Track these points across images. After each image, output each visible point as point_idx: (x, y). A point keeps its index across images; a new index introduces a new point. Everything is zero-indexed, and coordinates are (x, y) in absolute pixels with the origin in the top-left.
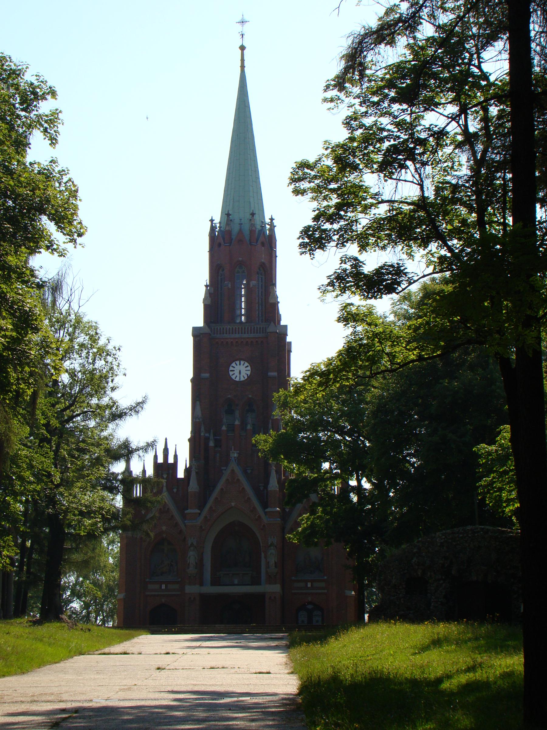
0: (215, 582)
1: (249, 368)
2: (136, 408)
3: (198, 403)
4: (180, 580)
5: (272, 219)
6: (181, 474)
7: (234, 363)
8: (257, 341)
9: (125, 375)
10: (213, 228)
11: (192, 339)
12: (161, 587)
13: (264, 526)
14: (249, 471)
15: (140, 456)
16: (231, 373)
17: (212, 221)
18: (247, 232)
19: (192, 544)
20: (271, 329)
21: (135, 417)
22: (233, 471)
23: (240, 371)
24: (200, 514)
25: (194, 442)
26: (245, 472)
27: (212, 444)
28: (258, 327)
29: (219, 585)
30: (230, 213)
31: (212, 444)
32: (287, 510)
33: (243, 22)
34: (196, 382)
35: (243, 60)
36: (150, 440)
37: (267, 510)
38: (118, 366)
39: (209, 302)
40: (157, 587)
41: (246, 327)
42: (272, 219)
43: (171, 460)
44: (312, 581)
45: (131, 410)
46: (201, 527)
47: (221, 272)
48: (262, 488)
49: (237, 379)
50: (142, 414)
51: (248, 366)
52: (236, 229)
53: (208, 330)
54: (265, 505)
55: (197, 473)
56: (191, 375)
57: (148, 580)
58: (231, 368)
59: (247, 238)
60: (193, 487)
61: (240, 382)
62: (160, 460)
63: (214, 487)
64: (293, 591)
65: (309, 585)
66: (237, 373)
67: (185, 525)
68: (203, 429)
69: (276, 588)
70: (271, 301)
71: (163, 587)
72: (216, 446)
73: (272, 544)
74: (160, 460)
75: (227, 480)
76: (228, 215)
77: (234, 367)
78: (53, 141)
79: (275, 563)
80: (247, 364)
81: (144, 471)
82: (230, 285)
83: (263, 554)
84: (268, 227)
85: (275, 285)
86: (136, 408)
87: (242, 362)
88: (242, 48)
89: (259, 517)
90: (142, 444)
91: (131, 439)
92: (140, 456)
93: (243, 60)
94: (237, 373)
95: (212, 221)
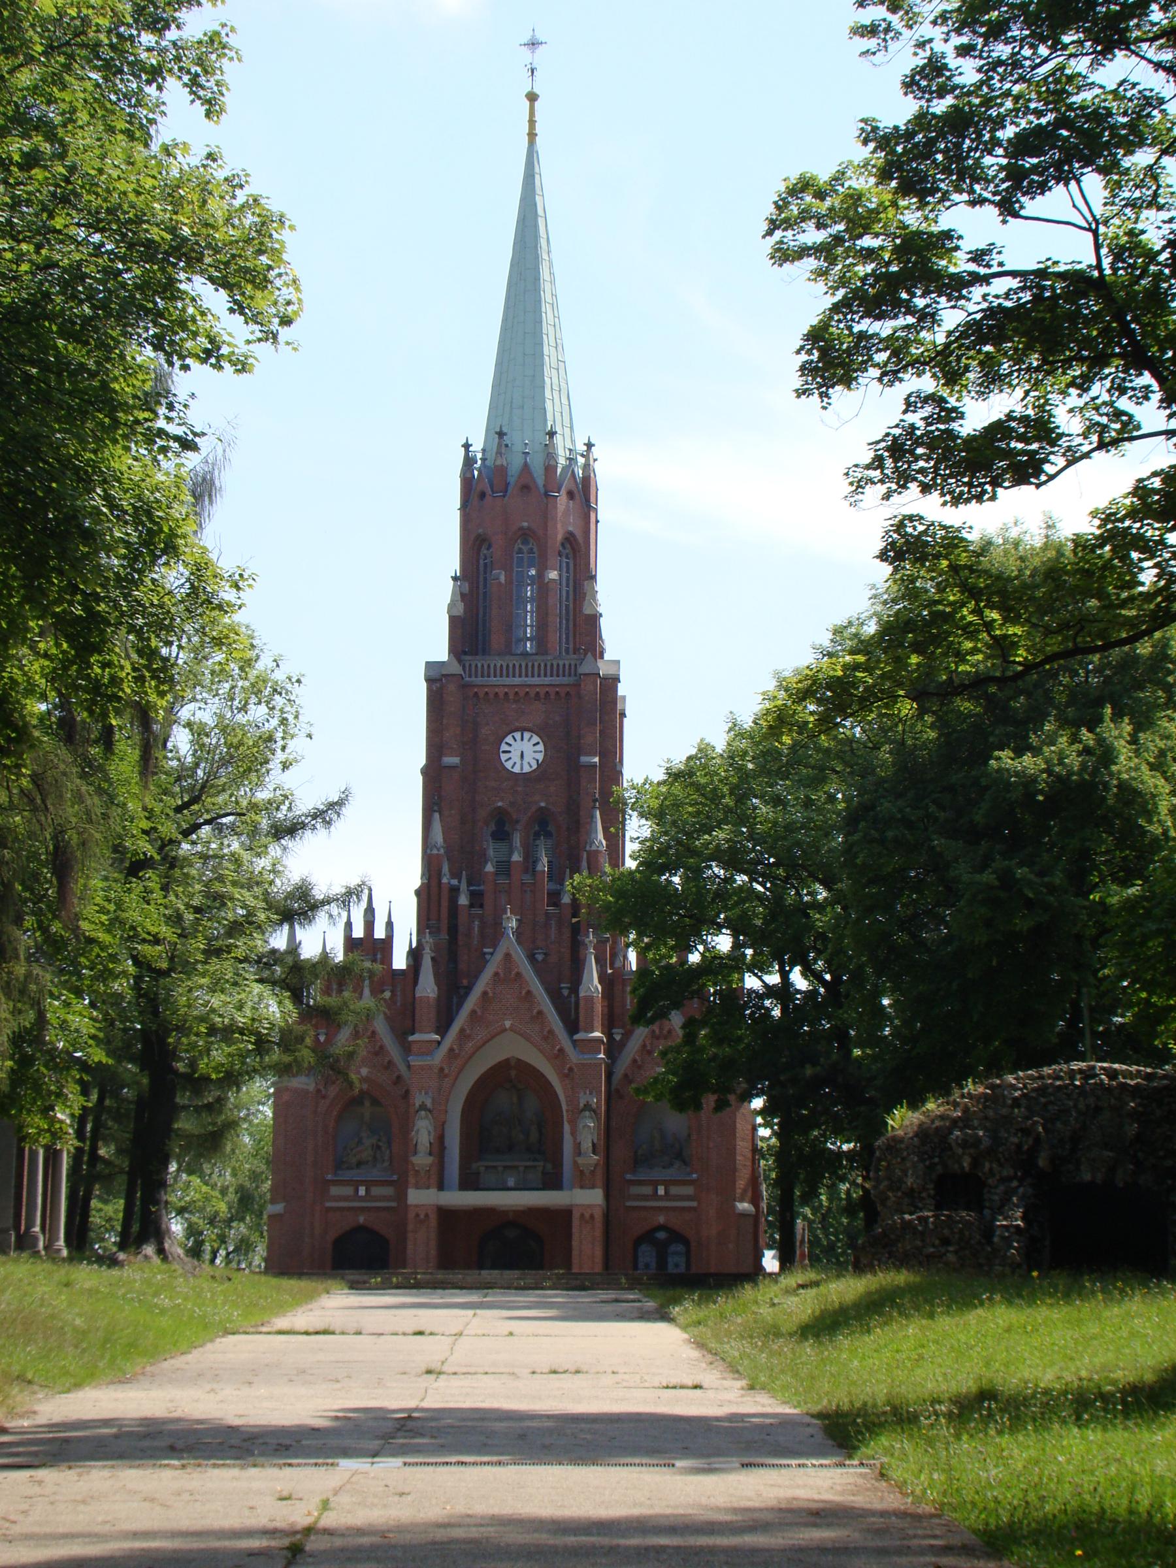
0: (469, 1182)
1: (541, 747)
2: (325, 815)
3: (437, 815)
4: (395, 1177)
5: (589, 446)
6: (400, 961)
9: (310, 736)
10: (469, 462)
11: (424, 685)
12: (357, 1191)
13: (571, 1069)
14: (540, 957)
15: (331, 916)
16: (504, 757)
17: (467, 446)
19: (423, 1107)
20: (584, 669)
21: (322, 832)
22: (508, 956)
23: (523, 753)
24: (439, 1043)
25: (428, 897)
26: (531, 958)
27: (463, 900)
29: (477, 1188)
30: (505, 430)
31: (463, 900)
32: (618, 1038)
33: (533, 44)
34: (433, 775)
35: (532, 122)
36: (353, 882)
37: (576, 1037)
38: (296, 717)
39: (460, 610)
40: (348, 1191)
42: (589, 446)
43: (380, 933)
44: (667, 1184)
45: (315, 817)
46: (441, 1069)
47: (484, 551)
48: (566, 992)
49: (517, 770)
50: (339, 826)
52: (515, 464)
53: (456, 669)
54: (573, 1027)
55: (433, 959)
56: (422, 761)
57: (329, 1177)
58: (504, 747)
59: (540, 481)
60: (428, 987)
62: (358, 932)
63: (469, 989)
64: (628, 1204)
65: (661, 1191)
66: (515, 757)
67: (409, 1067)
68: (446, 869)
69: (593, 1197)
70: (587, 611)
71: (362, 1191)
72: (471, 905)
73: (587, 1107)
74: (358, 932)
75: (496, 974)
76: (501, 434)
78: (213, 108)
79: (594, 1145)
80: (536, 739)
82: (502, 579)
83: (567, 1127)
84: (581, 460)
85: (593, 578)
86: (325, 815)
87: (527, 735)
88: (532, 97)
89: (561, 1050)
90: (338, 890)
91: (313, 880)
92: (331, 916)
93: (532, 122)
94: (515, 757)
95: (467, 446)
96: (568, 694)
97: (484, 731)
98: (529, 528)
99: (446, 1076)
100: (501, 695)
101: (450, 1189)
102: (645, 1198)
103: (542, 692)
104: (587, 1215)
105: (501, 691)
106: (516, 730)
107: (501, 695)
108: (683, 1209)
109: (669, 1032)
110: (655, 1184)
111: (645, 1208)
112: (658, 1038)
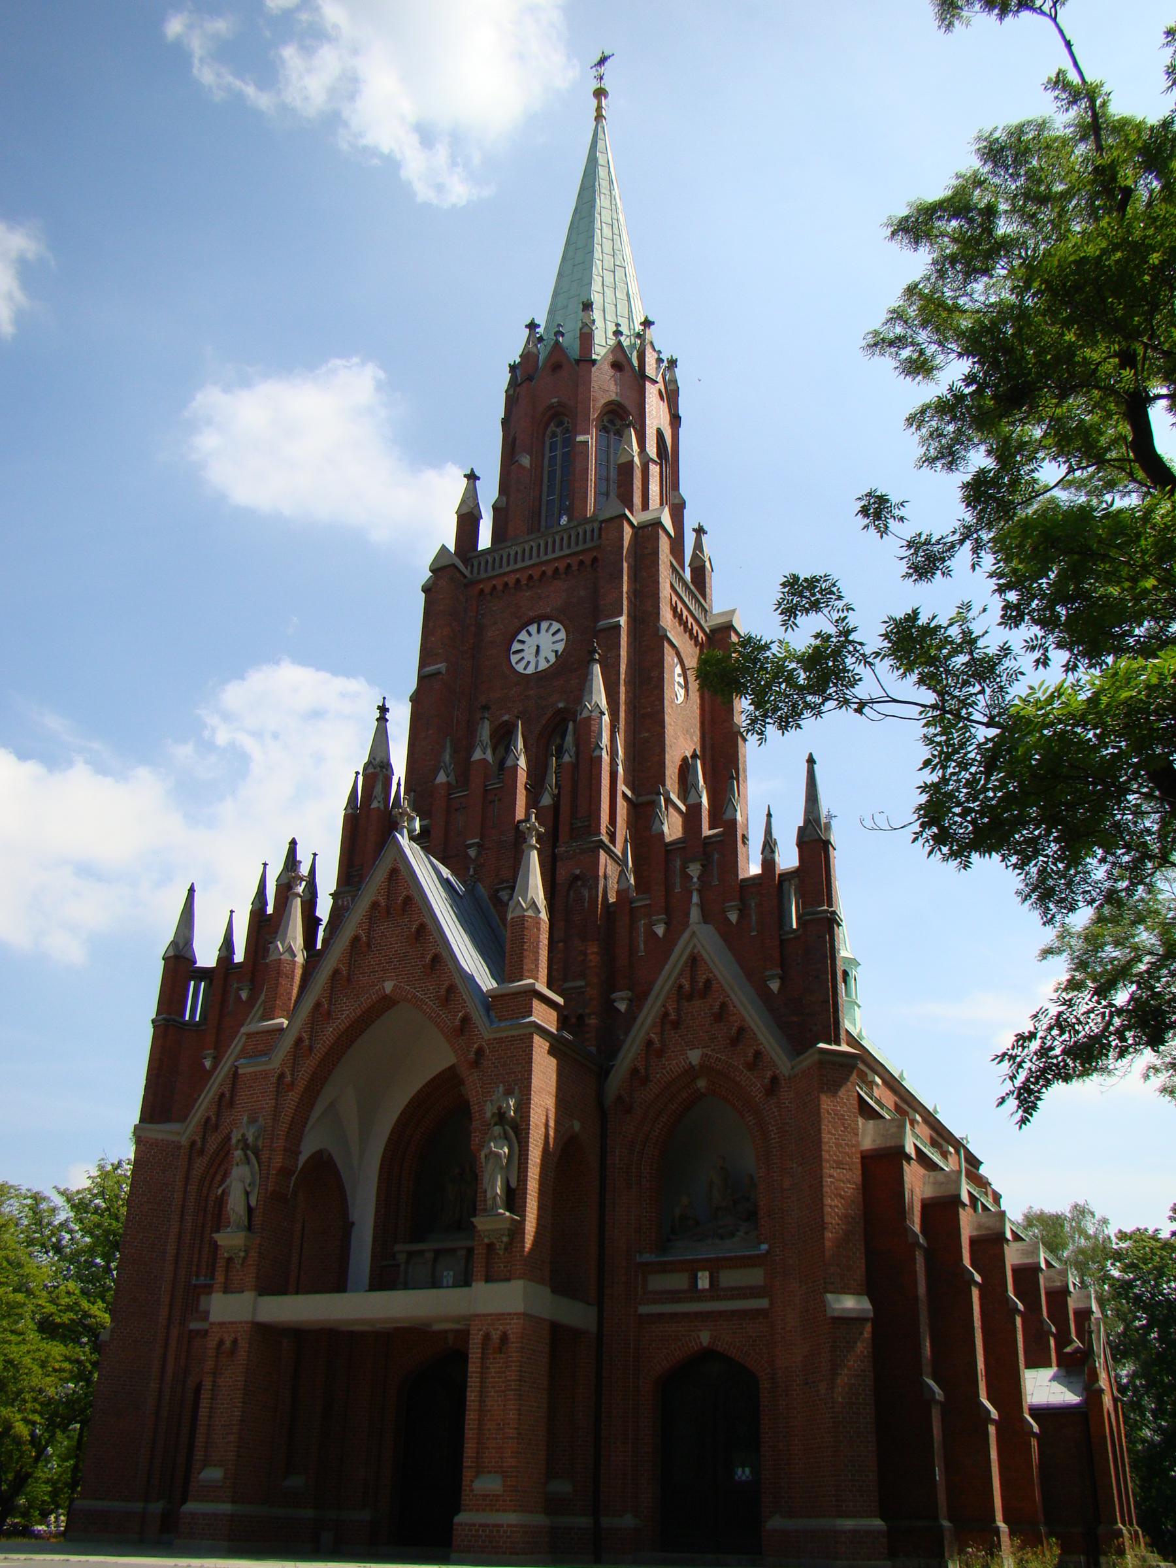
1: (562, 635)
7: (524, 632)
8: (581, 563)
13: (480, 1052)
16: (514, 659)
18: (570, 342)
28: (588, 527)
32: (622, 1007)
33: (603, 61)
41: (557, 538)
44: (715, 1266)
46: (282, 1076)
51: (559, 630)
61: (539, 676)
64: (643, 1309)
65: (704, 1282)
66: (529, 654)
75: (375, 905)
77: (523, 642)
80: (556, 626)
87: (544, 625)
93: (599, 108)
96: (595, 560)
98: (560, 404)
101: (355, 1290)
102: (674, 1296)
103: (561, 566)
104: (496, 1336)
106: (530, 623)
109: (708, 983)
110: (692, 1269)
111: (674, 1316)
112: (690, 997)
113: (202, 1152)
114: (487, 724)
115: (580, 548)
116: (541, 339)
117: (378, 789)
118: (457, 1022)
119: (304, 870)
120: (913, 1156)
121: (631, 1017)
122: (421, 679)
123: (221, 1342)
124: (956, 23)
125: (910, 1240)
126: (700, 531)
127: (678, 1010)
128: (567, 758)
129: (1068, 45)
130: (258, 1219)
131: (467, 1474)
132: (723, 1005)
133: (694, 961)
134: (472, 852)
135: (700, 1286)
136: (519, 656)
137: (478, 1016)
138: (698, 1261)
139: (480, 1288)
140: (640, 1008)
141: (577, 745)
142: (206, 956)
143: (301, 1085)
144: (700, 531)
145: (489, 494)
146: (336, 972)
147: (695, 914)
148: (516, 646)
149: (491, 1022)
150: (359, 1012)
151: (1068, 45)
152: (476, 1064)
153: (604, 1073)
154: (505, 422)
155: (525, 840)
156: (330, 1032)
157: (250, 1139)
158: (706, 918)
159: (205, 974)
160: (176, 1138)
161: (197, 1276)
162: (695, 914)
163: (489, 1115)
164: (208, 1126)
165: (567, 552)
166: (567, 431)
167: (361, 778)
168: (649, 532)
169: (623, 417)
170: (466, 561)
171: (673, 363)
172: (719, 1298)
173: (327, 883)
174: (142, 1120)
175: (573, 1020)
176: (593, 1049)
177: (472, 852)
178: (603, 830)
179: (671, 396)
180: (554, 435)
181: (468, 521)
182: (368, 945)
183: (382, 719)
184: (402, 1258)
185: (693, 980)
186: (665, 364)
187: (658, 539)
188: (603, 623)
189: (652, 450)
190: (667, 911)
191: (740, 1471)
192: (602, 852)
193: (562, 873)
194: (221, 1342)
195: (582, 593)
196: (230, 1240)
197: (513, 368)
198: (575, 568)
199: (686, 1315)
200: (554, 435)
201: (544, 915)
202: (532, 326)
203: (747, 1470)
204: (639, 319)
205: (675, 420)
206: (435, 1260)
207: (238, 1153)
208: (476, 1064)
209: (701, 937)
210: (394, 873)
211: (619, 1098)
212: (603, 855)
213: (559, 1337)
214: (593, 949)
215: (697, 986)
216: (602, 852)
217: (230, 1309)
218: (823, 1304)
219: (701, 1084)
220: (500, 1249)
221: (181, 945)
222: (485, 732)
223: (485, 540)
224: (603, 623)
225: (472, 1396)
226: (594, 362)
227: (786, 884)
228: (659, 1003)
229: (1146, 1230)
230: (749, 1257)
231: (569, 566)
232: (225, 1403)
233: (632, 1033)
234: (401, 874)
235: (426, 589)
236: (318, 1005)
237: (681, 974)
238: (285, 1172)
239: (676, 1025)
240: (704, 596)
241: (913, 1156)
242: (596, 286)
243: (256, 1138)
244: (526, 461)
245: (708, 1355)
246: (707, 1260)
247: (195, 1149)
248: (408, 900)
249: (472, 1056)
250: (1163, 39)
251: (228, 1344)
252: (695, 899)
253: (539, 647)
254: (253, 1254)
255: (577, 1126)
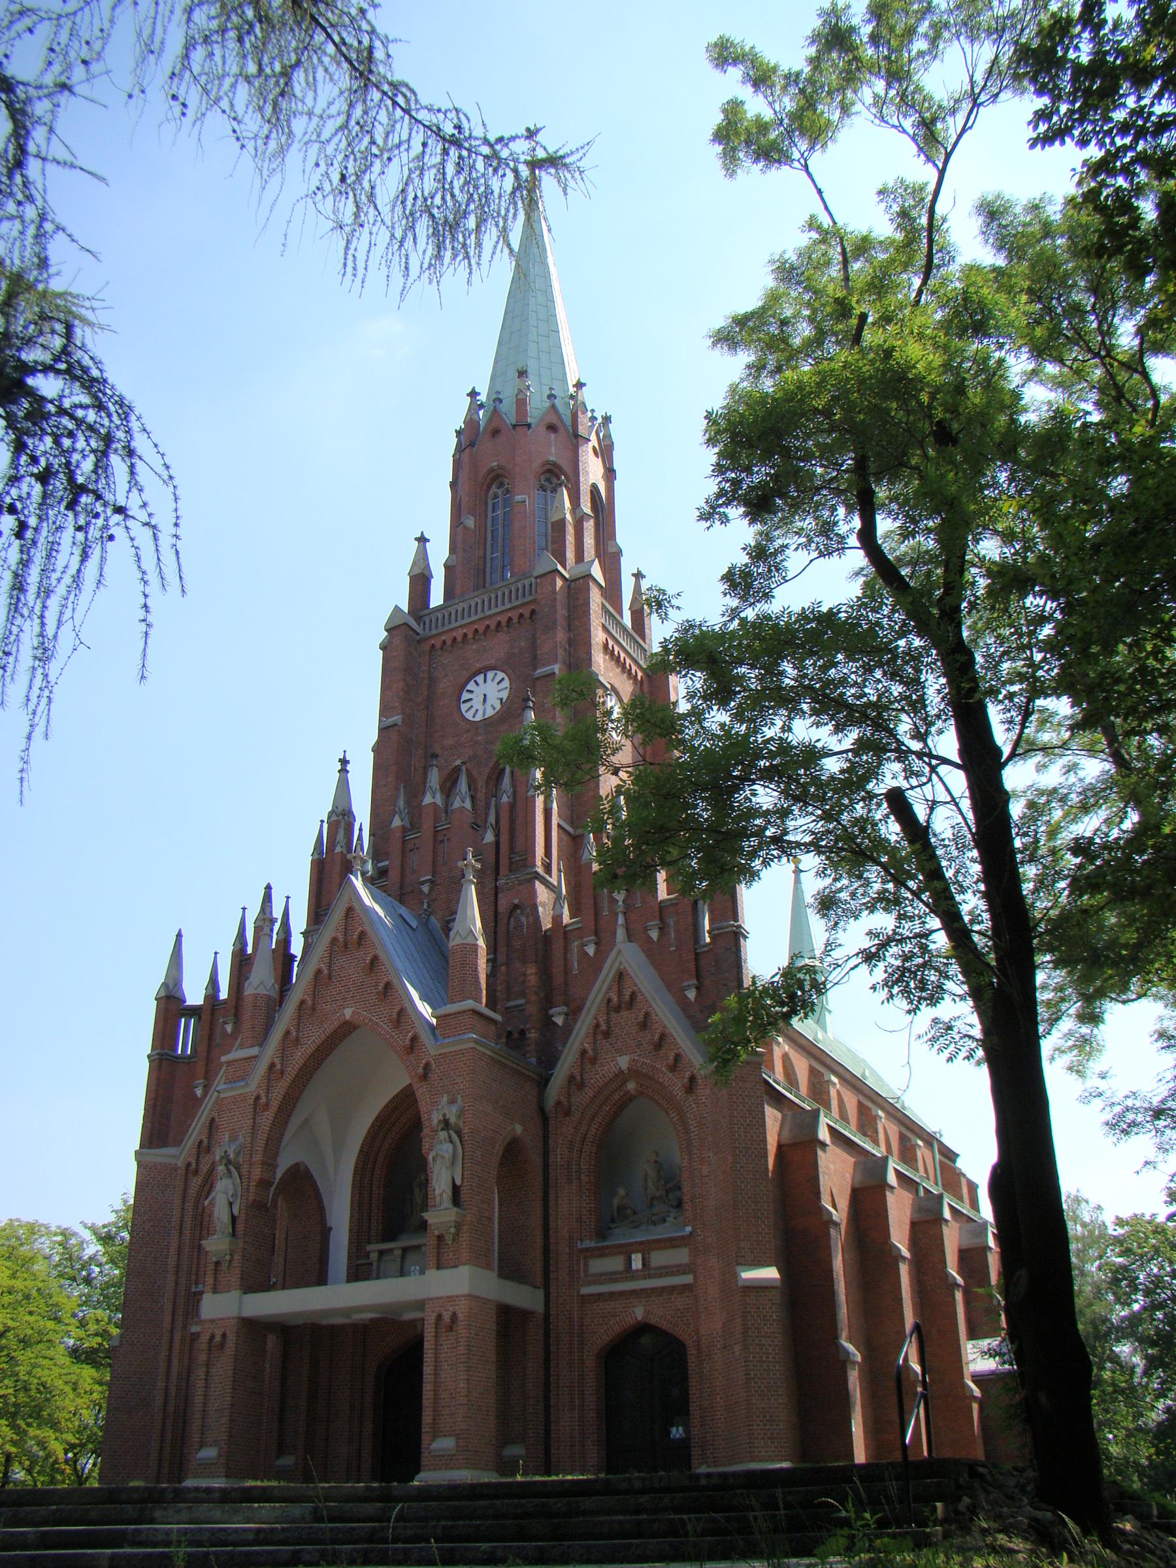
1: (506, 683)
7: (472, 682)
13: (427, 1066)
16: (464, 707)
18: (508, 408)
28: (527, 582)
32: (559, 1021)
41: (500, 593)
42: (579, 385)
46: (258, 1098)
49: (479, 718)
61: (487, 722)
64: (585, 1290)
65: (637, 1263)
66: (477, 703)
75: (334, 940)
77: (471, 692)
79: (456, 1189)
80: (501, 675)
81: (214, 982)
87: (490, 675)
96: (533, 612)
97: (443, 685)
98: (500, 467)
99: (267, 1106)
100: (459, 639)
102: (612, 1277)
103: (503, 619)
104: (447, 1317)
105: (458, 635)
107: (459, 639)
108: (672, 1289)
109: (633, 995)
110: (626, 1251)
111: (612, 1295)
112: (618, 1009)
113: (196, 1172)
114: (435, 770)
115: (518, 603)
116: (481, 406)
117: (341, 833)
118: (407, 1042)
119: (277, 913)
120: (828, 1141)
121: (568, 1029)
122: (382, 730)
123: (213, 1337)
124: (739, 171)
125: (825, 1218)
126: (638, 576)
127: (608, 1021)
128: (505, 799)
129: (819, 192)
130: (240, 1227)
131: (425, 1439)
132: (647, 1015)
133: (621, 976)
134: (426, 889)
135: (634, 1267)
136: (468, 705)
137: (425, 1037)
138: (630, 1244)
139: (433, 1274)
140: (575, 1021)
141: (514, 786)
142: (194, 995)
143: (275, 1104)
144: (638, 576)
145: (439, 554)
146: (303, 1002)
147: (621, 933)
148: (465, 696)
149: (436, 1040)
150: (323, 1037)
151: (819, 192)
152: (425, 1077)
153: (543, 1082)
154: (454, 485)
155: (463, 876)
156: (299, 1057)
157: (232, 1156)
158: (630, 936)
159: (194, 1011)
160: (173, 1161)
161: (197, 1284)
162: (621, 933)
163: (435, 1122)
164: (203, 1149)
165: (508, 606)
166: (508, 491)
167: (325, 826)
168: (579, 586)
169: (558, 475)
170: (419, 619)
171: (607, 419)
172: (650, 1277)
173: (299, 922)
174: (143, 1145)
175: (516, 1035)
176: (534, 1060)
177: (426, 889)
178: (539, 863)
179: (606, 451)
180: (496, 496)
181: (420, 582)
182: (330, 977)
183: (344, 771)
184: (374, 1256)
185: (620, 993)
186: (600, 420)
187: (588, 590)
188: (540, 672)
189: (586, 507)
190: (596, 933)
191: (674, 1430)
192: (537, 883)
193: (504, 904)
194: (213, 1337)
195: (523, 644)
196: (217, 1244)
197: (458, 433)
198: (515, 621)
199: (622, 1294)
200: (496, 496)
201: (481, 943)
202: (473, 394)
203: (681, 1429)
204: (572, 381)
205: (610, 474)
206: (403, 1257)
207: (221, 1168)
208: (425, 1077)
209: (627, 955)
210: (350, 910)
211: (559, 1103)
212: (539, 887)
213: (508, 1319)
214: (531, 970)
215: (624, 1000)
216: (537, 883)
217: (222, 1306)
218: (736, 1276)
219: (631, 1086)
220: (449, 1239)
221: (171, 986)
222: (434, 778)
223: (437, 598)
224: (540, 672)
225: (428, 1369)
226: (529, 426)
227: (700, 903)
228: (590, 1017)
229: (1143, 1215)
230: (675, 1239)
231: (510, 619)
232: (217, 1391)
233: (568, 1046)
234: (353, 911)
235: (384, 647)
236: (288, 1033)
237: (609, 989)
238: (264, 1184)
239: (607, 1034)
240: (643, 638)
241: (828, 1141)
242: (532, 353)
243: (238, 1154)
244: (470, 522)
245: (644, 1328)
246: (641, 1243)
247: (190, 1171)
248: (363, 935)
249: (420, 1071)
250: (876, 199)
251: (218, 1338)
252: (621, 920)
253: (486, 696)
254: (237, 1257)
255: (519, 1129)
